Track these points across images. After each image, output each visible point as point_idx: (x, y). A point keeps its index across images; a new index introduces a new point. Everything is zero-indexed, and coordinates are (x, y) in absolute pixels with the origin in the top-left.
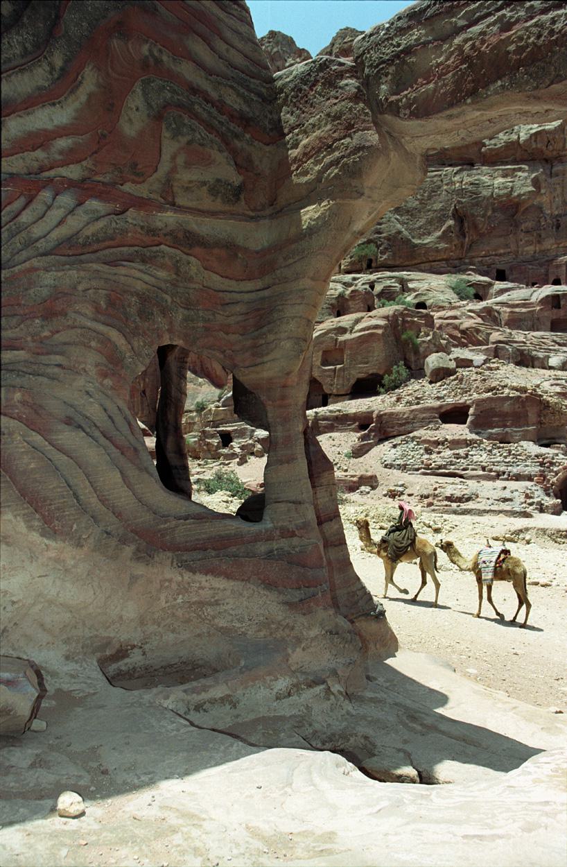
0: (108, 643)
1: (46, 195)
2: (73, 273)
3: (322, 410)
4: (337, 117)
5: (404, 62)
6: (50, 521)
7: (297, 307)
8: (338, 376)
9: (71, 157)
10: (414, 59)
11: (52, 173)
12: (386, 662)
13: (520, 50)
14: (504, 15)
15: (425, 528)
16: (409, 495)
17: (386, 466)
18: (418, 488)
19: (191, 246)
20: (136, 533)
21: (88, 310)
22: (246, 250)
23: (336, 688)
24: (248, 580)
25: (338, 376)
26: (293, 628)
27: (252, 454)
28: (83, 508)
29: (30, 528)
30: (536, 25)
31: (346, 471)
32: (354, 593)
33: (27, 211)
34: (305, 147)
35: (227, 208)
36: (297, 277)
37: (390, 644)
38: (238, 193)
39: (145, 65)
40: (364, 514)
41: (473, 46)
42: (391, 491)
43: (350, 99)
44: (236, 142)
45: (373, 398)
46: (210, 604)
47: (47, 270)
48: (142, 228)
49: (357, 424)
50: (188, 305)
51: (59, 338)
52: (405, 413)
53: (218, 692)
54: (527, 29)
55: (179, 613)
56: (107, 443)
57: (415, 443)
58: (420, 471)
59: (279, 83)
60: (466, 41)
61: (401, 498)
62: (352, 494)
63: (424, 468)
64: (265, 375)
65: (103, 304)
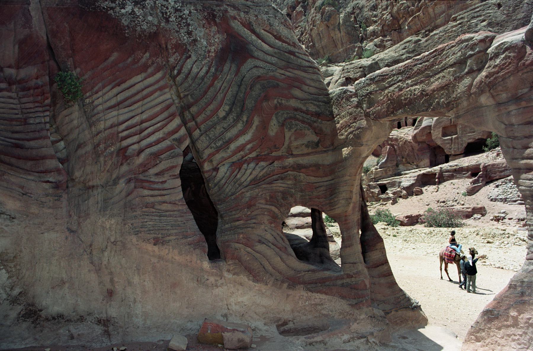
0: (280, 319)
1: (245, 166)
2: (257, 190)
3: (445, 166)
4: (351, 114)
5: (370, 97)
6: (256, 277)
7: (345, 187)
8: (455, 143)
9: (252, 150)
10: (372, 96)
11: (246, 157)
12: (419, 330)
13: (406, 99)
14: (399, 85)
15: (521, 242)
16: (510, 219)
17: (492, 200)
18: (516, 214)
19: (300, 169)
20: (288, 279)
21: (263, 201)
22: (323, 165)
23: (372, 340)
24: (334, 295)
25: (455, 143)
26: (353, 315)
27: (401, 197)
28: (267, 272)
29: (249, 279)
30: (409, 91)
31: (463, 205)
32: (398, 298)
33: (239, 173)
34: (341, 124)
35: (313, 150)
36: (343, 176)
37: (424, 322)
38: (317, 144)
39: (276, 108)
40: (476, 233)
41: (391, 95)
42: (496, 217)
43: (355, 107)
44: (315, 124)
45: (480, 155)
46: (320, 305)
47: (247, 192)
48: (280, 167)
49: (470, 173)
50: (302, 191)
51: (254, 213)
52: (503, 164)
53: (319, 338)
54: (407, 92)
55: (307, 308)
56: (274, 247)
57: (512, 183)
58: (517, 202)
59: (331, 96)
60: (389, 92)
61: (504, 221)
62: (468, 220)
63: (520, 200)
64: (336, 212)
65: (268, 198)
